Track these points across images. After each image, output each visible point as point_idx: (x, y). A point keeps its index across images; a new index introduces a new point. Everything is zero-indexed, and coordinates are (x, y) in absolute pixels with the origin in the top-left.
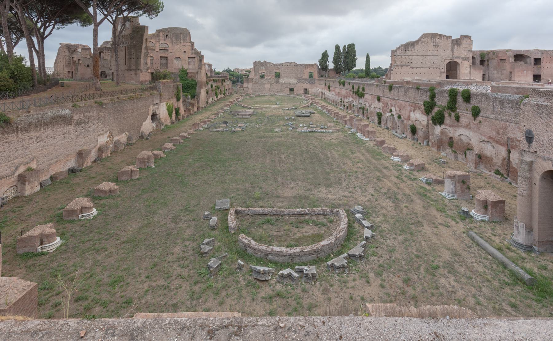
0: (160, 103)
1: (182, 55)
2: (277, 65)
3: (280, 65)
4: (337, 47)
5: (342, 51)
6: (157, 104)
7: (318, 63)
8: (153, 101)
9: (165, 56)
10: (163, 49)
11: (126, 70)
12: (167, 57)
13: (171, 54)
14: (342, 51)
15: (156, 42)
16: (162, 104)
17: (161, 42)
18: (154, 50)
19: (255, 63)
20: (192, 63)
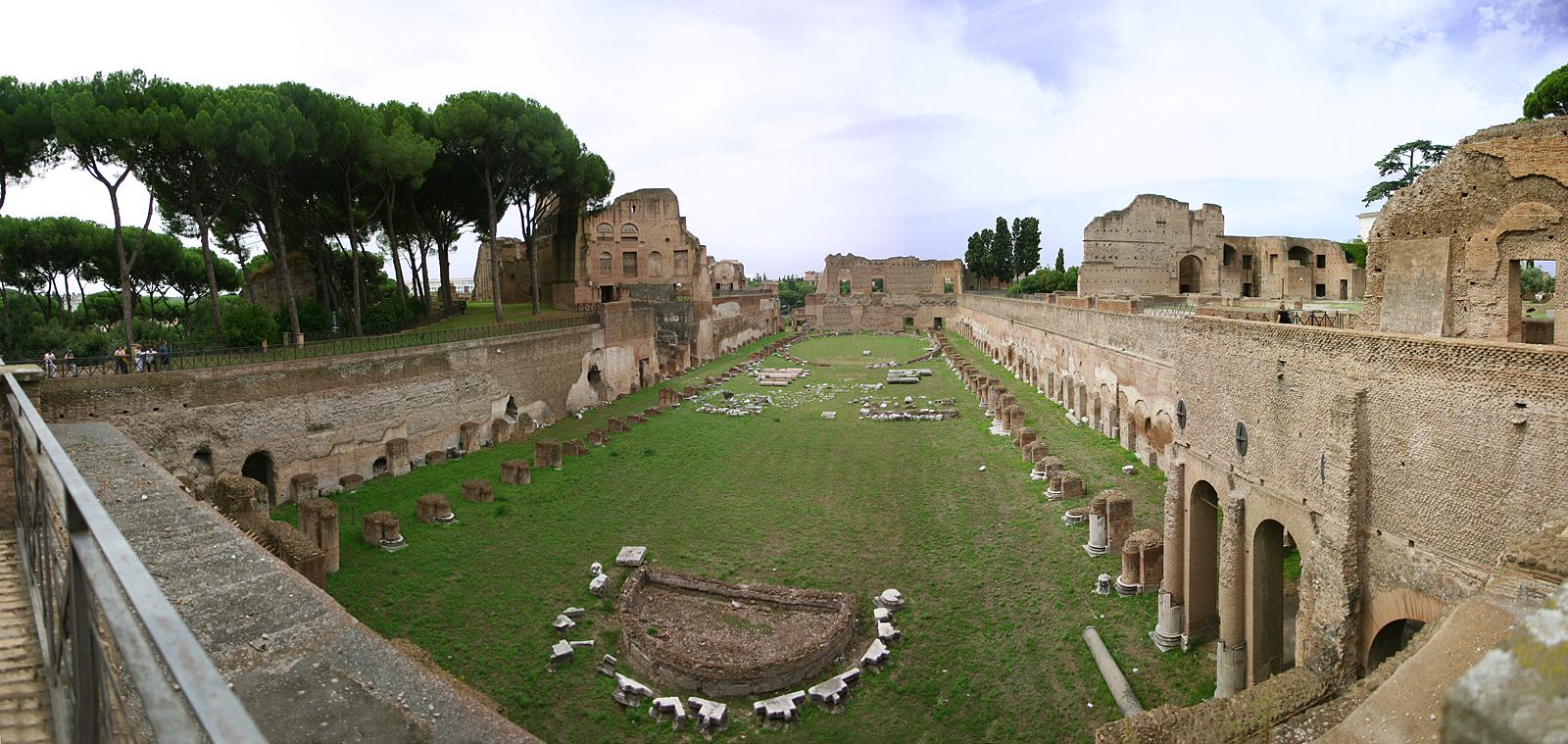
0: (606, 347)
1: (662, 247)
2: (876, 262)
3: (882, 262)
4: (1002, 223)
5: (1011, 231)
6: (598, 349)
7: (963, 259)
8: (590, 344)
9: (632, 250)
10: (628, 235)
11: (554, 282)
12: (635, 253)
13: (642, 246)
14: (1011, 231)
15: (614, 222)
16: (608, 349)
17: (623, 224)
18: (612, 239)
19: (830, 259)
20: (682, 263)
